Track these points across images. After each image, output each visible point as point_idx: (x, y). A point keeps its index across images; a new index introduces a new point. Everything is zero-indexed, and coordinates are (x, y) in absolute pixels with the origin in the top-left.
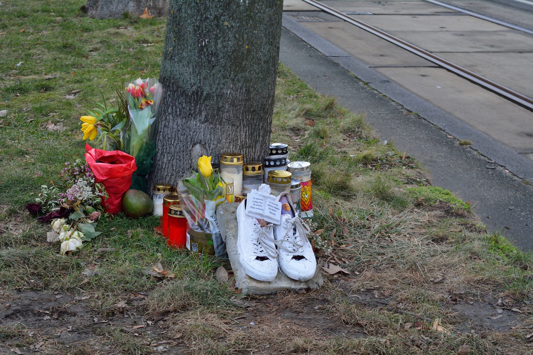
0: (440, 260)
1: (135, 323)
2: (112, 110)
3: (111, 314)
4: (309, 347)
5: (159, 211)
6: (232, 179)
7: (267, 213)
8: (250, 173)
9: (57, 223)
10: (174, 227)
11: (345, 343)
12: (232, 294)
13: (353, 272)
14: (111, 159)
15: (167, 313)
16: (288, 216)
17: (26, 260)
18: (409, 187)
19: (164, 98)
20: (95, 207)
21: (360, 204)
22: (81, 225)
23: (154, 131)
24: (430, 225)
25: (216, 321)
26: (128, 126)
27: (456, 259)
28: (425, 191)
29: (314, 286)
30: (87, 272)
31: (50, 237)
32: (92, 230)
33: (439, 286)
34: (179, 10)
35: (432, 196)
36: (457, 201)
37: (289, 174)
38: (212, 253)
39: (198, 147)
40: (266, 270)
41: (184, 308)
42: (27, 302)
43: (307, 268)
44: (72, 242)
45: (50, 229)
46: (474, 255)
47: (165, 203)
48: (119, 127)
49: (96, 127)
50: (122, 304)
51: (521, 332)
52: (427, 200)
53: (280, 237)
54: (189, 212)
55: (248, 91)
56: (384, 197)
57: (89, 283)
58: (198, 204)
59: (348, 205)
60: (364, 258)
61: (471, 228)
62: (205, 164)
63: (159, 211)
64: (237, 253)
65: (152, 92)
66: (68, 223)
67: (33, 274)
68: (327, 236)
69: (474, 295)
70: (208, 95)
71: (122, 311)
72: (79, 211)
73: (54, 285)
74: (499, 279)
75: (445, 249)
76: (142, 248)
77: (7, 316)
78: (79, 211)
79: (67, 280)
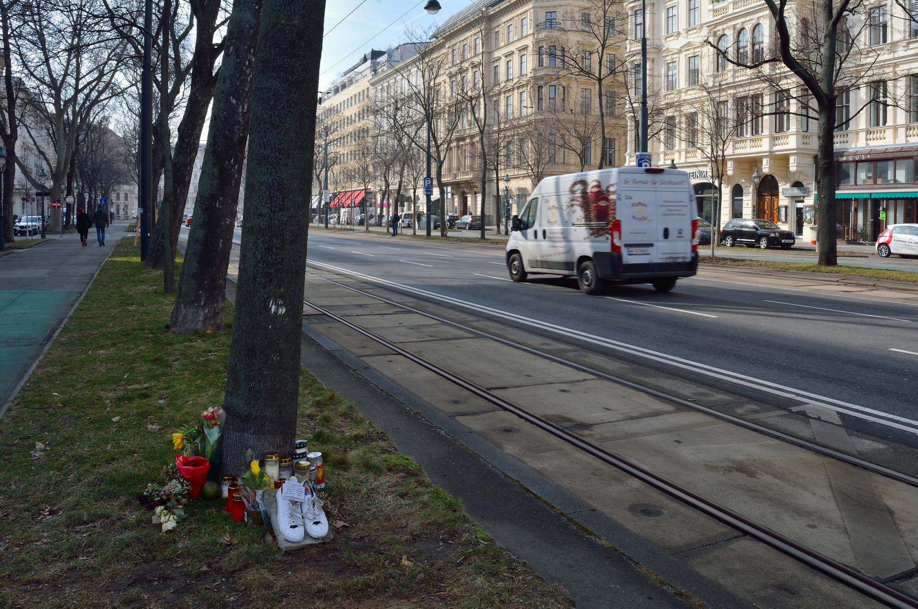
0: (405, 510)
1: (214, 581)
2: (194, 429)
3: (199, 576)
4: (326, 587)
5: (226, 494)
6: (272, 471)
7: (296, 496)
8: (284, 464)
9: (159, 509)
10: (235, 507)
11: (349, 582)
12: (275, 552)
13: (351, 524)
14: (194, 463)
15: (234, 572)
16: (309, 496)
17: (139, 540)
18: (383, 456)
19: (227, 420)
20: (184, 496)
21: (353, 473)
22: (175, 510)
23: (220, 441)
24: (396, 485)
25: (267, 574)
26: (204, 439)
27: (414, 509)
28: (393, 459)
29: (327, 540)
30: (180, 545)
31: (155, 520)
32: (182, 513)
33: (405, 530)
34: (236, 365)
35: (398, 462)
36: (413, 464)
37: (308, 463)
38: (261, 523)
39: (249, 450)
40: (296, 535)
41: (246, 567)
42: (141, 572)
43: (321, 530)
44: (169, 524)
45: (154, 514)
46: (425, 505)
47: (229, 490)
48: (198, 440)
49: (182, 440)
50: (205, 568)
51: (454, 559)
52: (395, 465)
53: (304, 511)
54: (245, 497)
55: (280, 412)
56: (368, 467)
57: (182, 554)
58: (252, 493)
59: (347, 475)
60: (358, 514)
61: (421, 483)
62: (255, 466)
63: (226, 494)
64: (278, 525)
65: (219, 416)
66: (166, 509)
67: (144, 550)
68: (333, 499)
69: (426, 534)
70: (255, 417)
71: (205, 573)
72: (173, 500)
73: (160, 557)
74: (440, 520)
75: (407, 502)
76: (215, 523)
77: (129, 585)
78: (173, 500)
79: (167, 553)
